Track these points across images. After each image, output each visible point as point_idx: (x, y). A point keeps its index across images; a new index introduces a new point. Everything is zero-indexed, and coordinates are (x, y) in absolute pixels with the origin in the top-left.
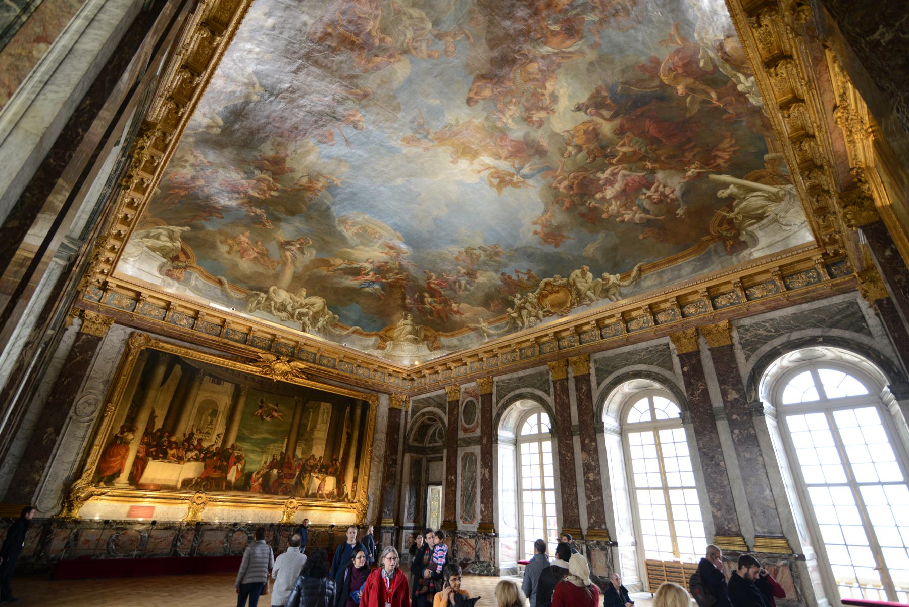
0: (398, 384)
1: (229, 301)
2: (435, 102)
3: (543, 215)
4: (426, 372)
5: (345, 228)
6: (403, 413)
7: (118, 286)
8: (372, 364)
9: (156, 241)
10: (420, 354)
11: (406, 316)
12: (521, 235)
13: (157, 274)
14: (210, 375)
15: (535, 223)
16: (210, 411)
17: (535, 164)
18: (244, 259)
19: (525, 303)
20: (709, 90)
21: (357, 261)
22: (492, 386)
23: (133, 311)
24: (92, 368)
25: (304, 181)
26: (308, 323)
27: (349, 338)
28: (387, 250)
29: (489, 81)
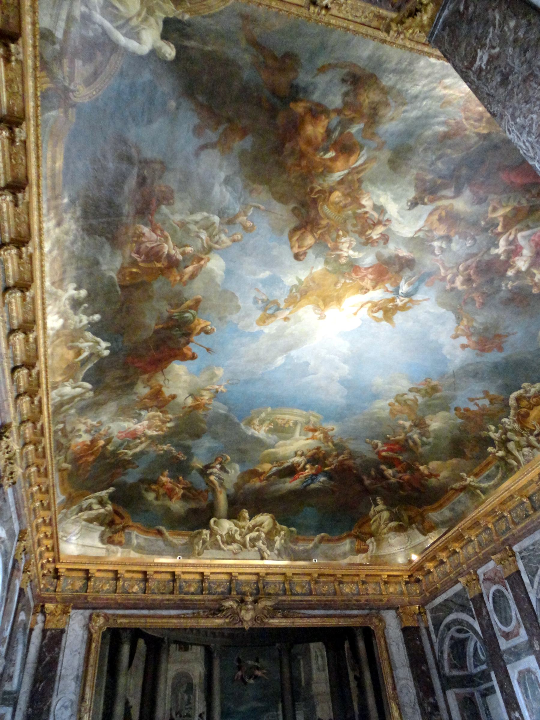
0: (402, 593)
1: (175, 551)
2: (265, 274)
3: (459, 324)
4: (430, 566)
5: (255, 429)
6: (424, 631)
7: (68, 570)
8: (358, 575)
9: (90, 512)
10: (414, 543)
11: (375, 501)
12: (448, 357)
13: (100, 545)
14: (176, 642)
15: (456, 337)
16: (184, 688)
17: (410, 277)
18: (174, 500)
19: (505, 433)
21: (287, 458)
22: (515, 561)
23: (86, 592)
24: (62, 666)
25: (190, 401)
26: (264, 547)
27: (319, 551)
28: (310, 434)
29: (303, 230)
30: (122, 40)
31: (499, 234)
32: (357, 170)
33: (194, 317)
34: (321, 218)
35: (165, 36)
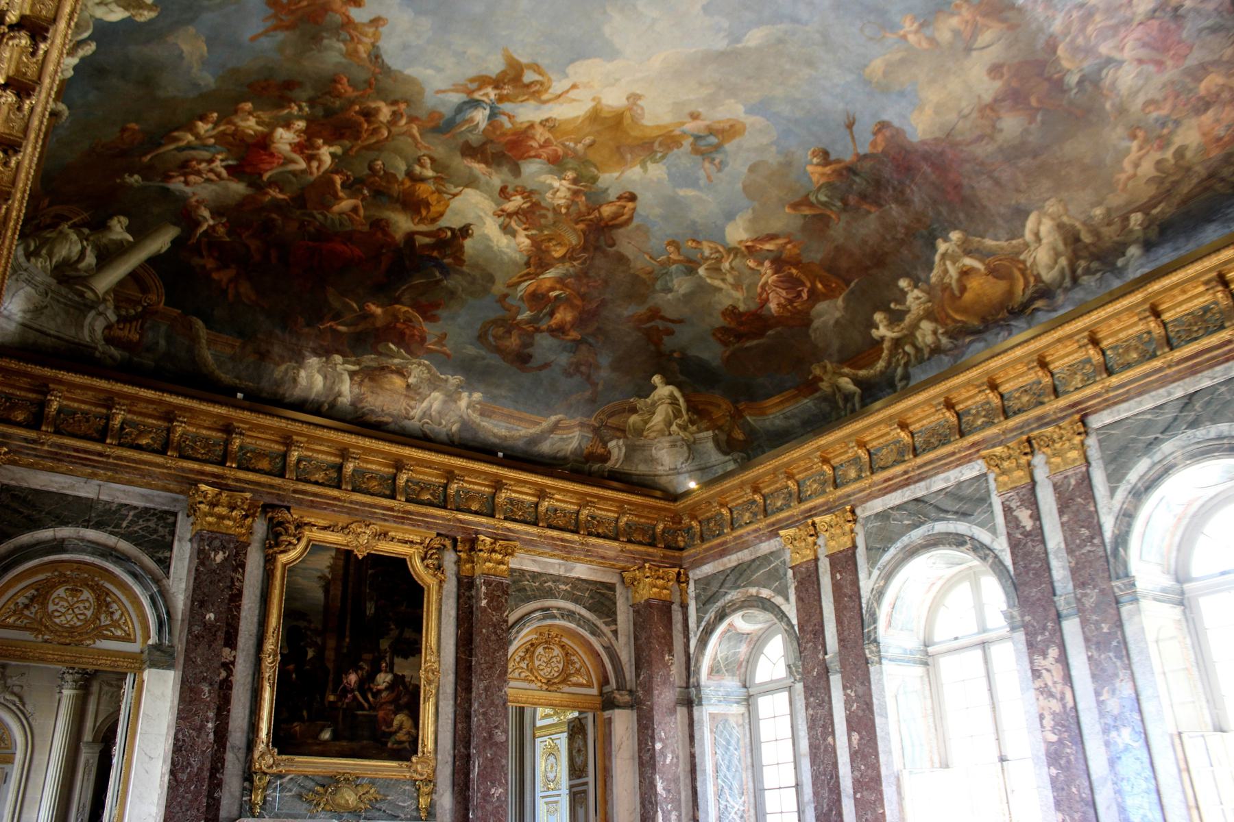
3: (373, 45)
15: (376, 22)
20: (352, 329)
29: (611, 223)
30: (681, 401)
31: (335, 170)
32: (528, 276)
33: (819, 188)
34: (584, 232)
35: (655, 388)
